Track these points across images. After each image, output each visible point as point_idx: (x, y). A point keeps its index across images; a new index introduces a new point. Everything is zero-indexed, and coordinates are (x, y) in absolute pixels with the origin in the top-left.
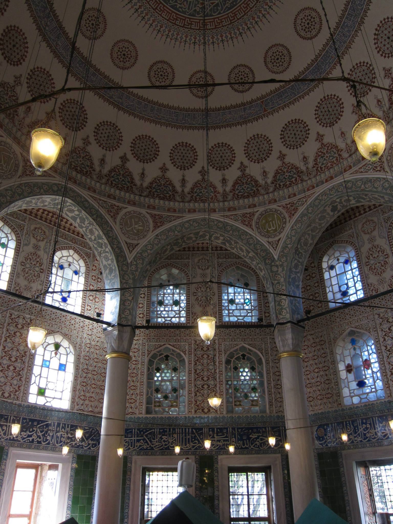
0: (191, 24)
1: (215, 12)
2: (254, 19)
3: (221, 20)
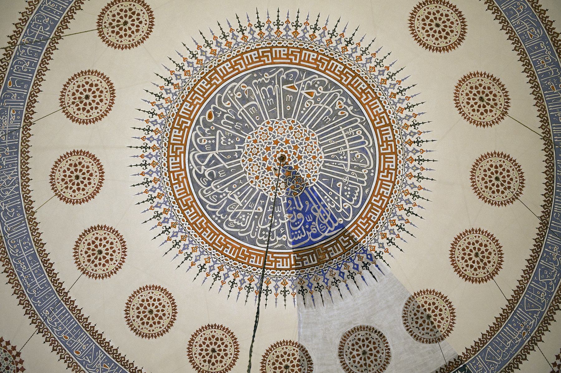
0: (342, 72)
1: (295, 73)
2: (228, 44)
3: (288, 58)
